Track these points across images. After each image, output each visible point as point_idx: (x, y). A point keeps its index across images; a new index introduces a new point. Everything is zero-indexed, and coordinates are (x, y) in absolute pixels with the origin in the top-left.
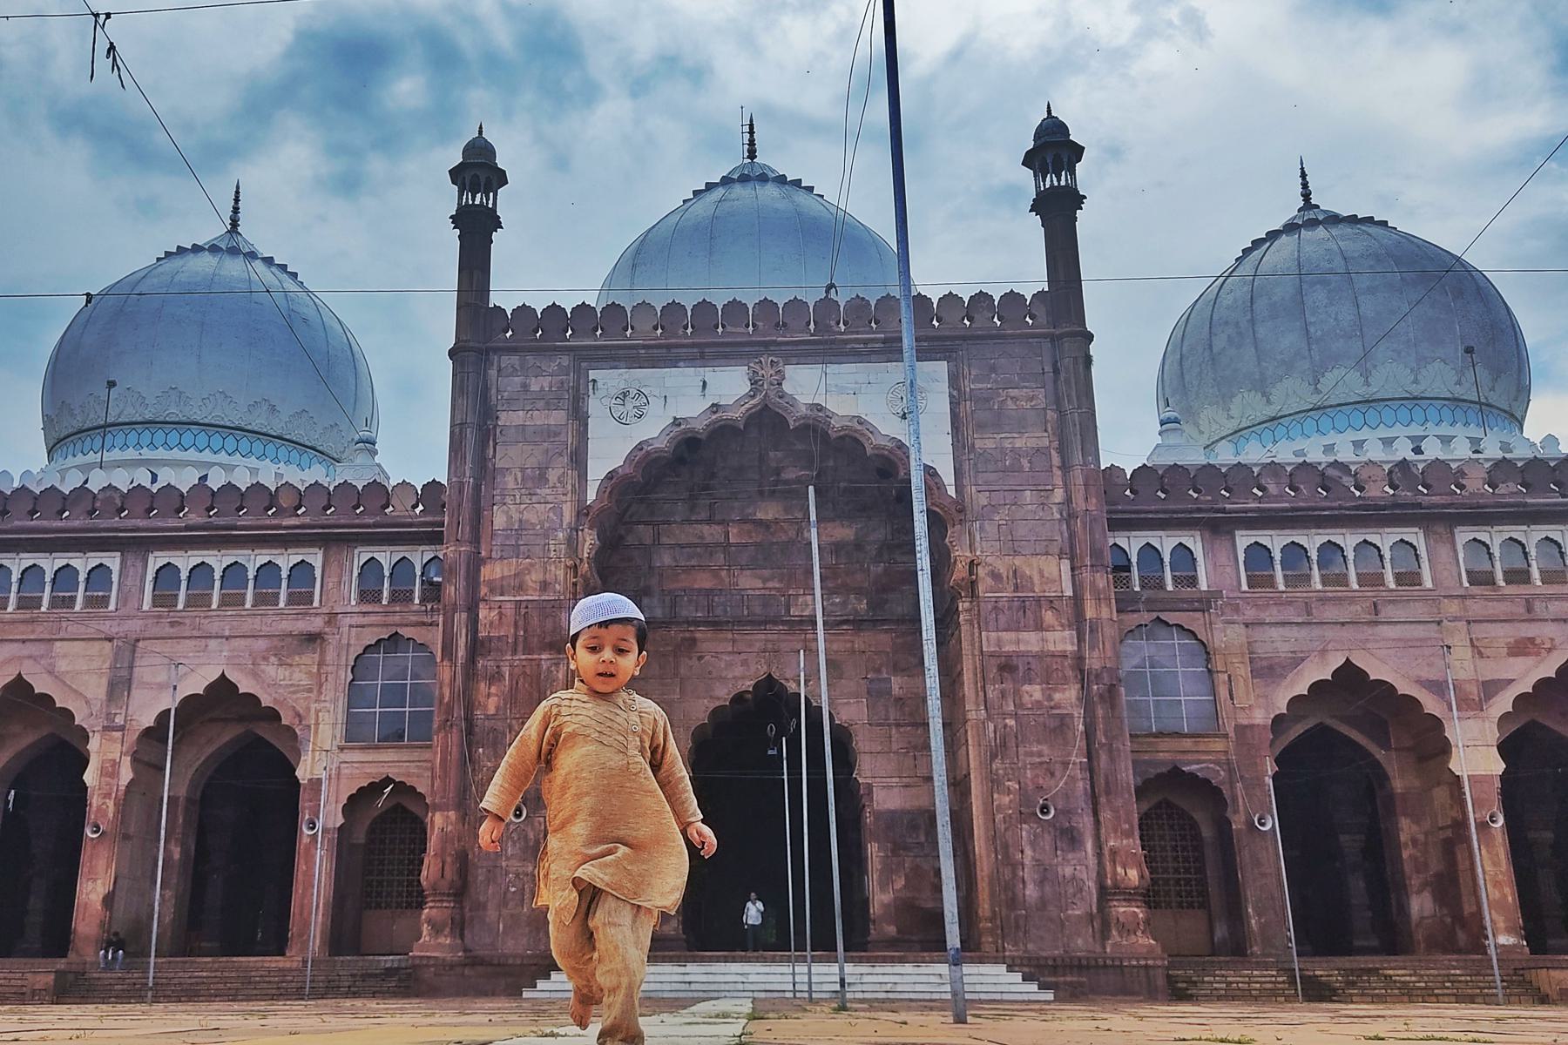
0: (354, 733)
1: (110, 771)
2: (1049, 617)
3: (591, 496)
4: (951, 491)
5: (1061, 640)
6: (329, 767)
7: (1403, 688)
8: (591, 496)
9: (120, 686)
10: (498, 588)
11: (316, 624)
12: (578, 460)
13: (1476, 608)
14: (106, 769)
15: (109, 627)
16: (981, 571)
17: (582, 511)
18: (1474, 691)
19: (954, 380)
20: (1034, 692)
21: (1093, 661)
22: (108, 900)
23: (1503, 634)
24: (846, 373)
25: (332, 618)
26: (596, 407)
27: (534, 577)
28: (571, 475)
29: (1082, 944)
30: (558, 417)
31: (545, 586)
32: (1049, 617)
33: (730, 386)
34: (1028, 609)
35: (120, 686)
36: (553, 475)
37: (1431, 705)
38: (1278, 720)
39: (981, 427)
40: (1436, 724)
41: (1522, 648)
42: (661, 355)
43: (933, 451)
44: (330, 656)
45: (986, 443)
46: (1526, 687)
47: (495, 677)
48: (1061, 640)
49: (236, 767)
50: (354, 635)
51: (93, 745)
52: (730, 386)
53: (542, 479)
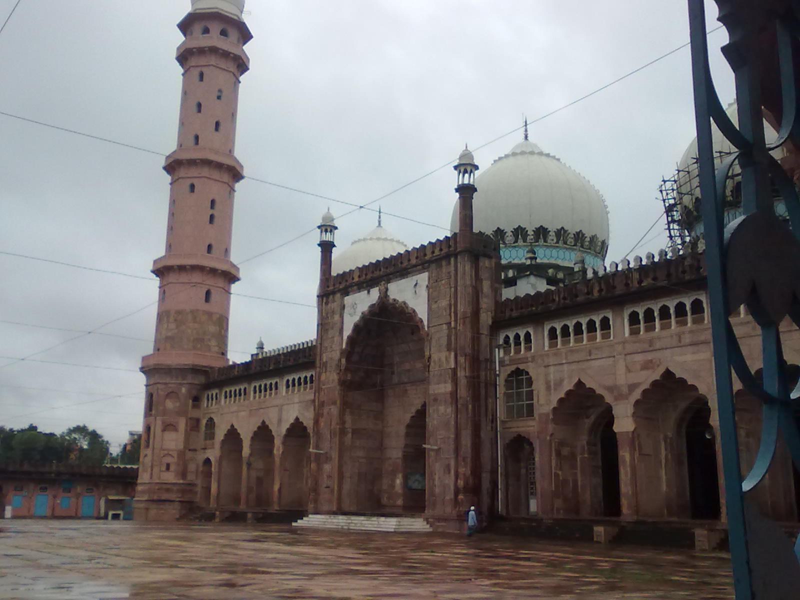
7: (599, 391)
9: (280, 421)
13: (630, 348)
18: (625, 390)
35: (280, 421)
37: (609, 399)
43: (422, 313)
45: (434, 306)
46: (646, 386)
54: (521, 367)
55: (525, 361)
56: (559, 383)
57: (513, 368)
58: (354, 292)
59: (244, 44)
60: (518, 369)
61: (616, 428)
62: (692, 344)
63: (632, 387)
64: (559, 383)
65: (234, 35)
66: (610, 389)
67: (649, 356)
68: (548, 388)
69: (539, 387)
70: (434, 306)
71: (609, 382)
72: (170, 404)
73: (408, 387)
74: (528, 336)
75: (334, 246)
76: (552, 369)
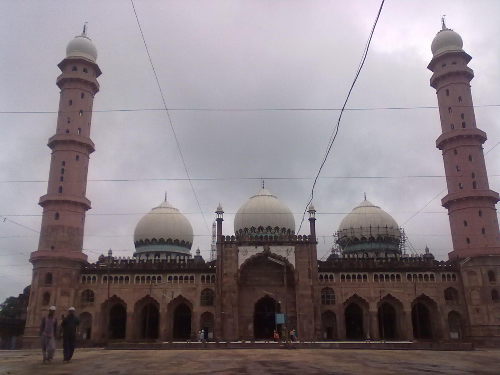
0: (202, 304)
3: (239, 268)
4: (295, 268)
6: (198, 309)
8: (239, 268)
11: (194, 286)
12: (238, 263)
14: (163, 310)
15: (162, 286)
17: (238, 270)
19: (296, 249)
22: (165, 330)
24: (279, 248)
25: (197, 285)
30: (233, 255)
33: (261, 249)
36: (233, 264)
37: (367, 301)
38: (344, 303)
40: (368, 304)
42: (250, 244)
43: (292, 260)
49: (182, 309)
50: (201, 288)
51: (161, 306)
52: (261, 249)
54: (329, 287)
55: (330, 285)
56: (346, 294)
57: (325, 287)
58: (246, 246)
59: (97, 77)
60: (327, 287)
61: (371, 310)
63: (376, 298)
65: (91, 72)
66: (368, 298)
67: (382, 289)
68: (342, 295)
69: (337, 294)
72: (65, 280)
75: (223, 220)
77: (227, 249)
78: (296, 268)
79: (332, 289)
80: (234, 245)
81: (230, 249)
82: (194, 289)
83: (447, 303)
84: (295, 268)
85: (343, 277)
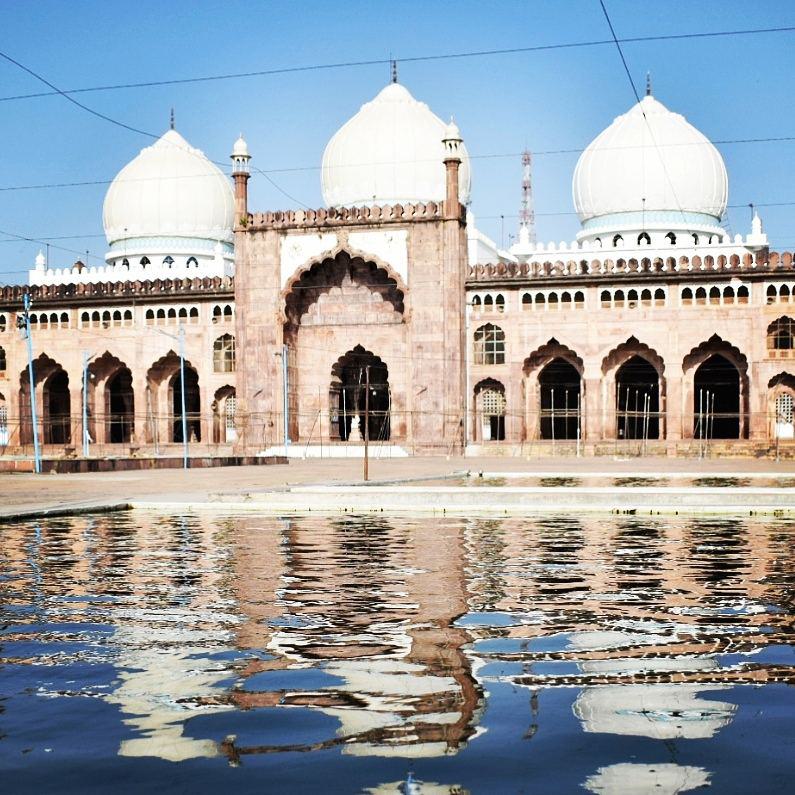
1: (140, 383)
2: (435, 328)
4: (405, 282)
5: (438, 337)
9: (139, 353)
10: (253, 321)
11: (198, 331)
12: (278, 273)
16: (414, 313)
18: (596, 349)
19: (408, 239)
20: (428, 355)
21: (447, 345)
23: (610, 326)
25: (205, 328)
26: (283, 252)
27: (264, 318)
28: (276, 279)
29: (437, 438)
30: (270, 257)
31: (268, 321)
32: (435, 328)
34: (427, 329)
35: (139, 353)
36: (269, 279)
39: (417, 258)
41: (616, 332)
44: (206, 342)
45: (417, 264)
47: (253, 353)
48: (438, 337)
53: (265, 280)
54: (493, 323)
56: (534, 338)
62: (655, 320)
64: (534, 338)
66: (582, 347)
67: (618, 325)
68: (522, 342)
70: (417, 264)
71: (582, 342)
73: (335, 329)
74: (500, 300)
76: (525, 327)
77: (256, 243)
78: (408, 282)
79: (498, 328)
80: (270, 234)
81: (262, 243)
82: (199, 336)
83: (773, 355)
84: (405, 282)
85: (527, 299)
